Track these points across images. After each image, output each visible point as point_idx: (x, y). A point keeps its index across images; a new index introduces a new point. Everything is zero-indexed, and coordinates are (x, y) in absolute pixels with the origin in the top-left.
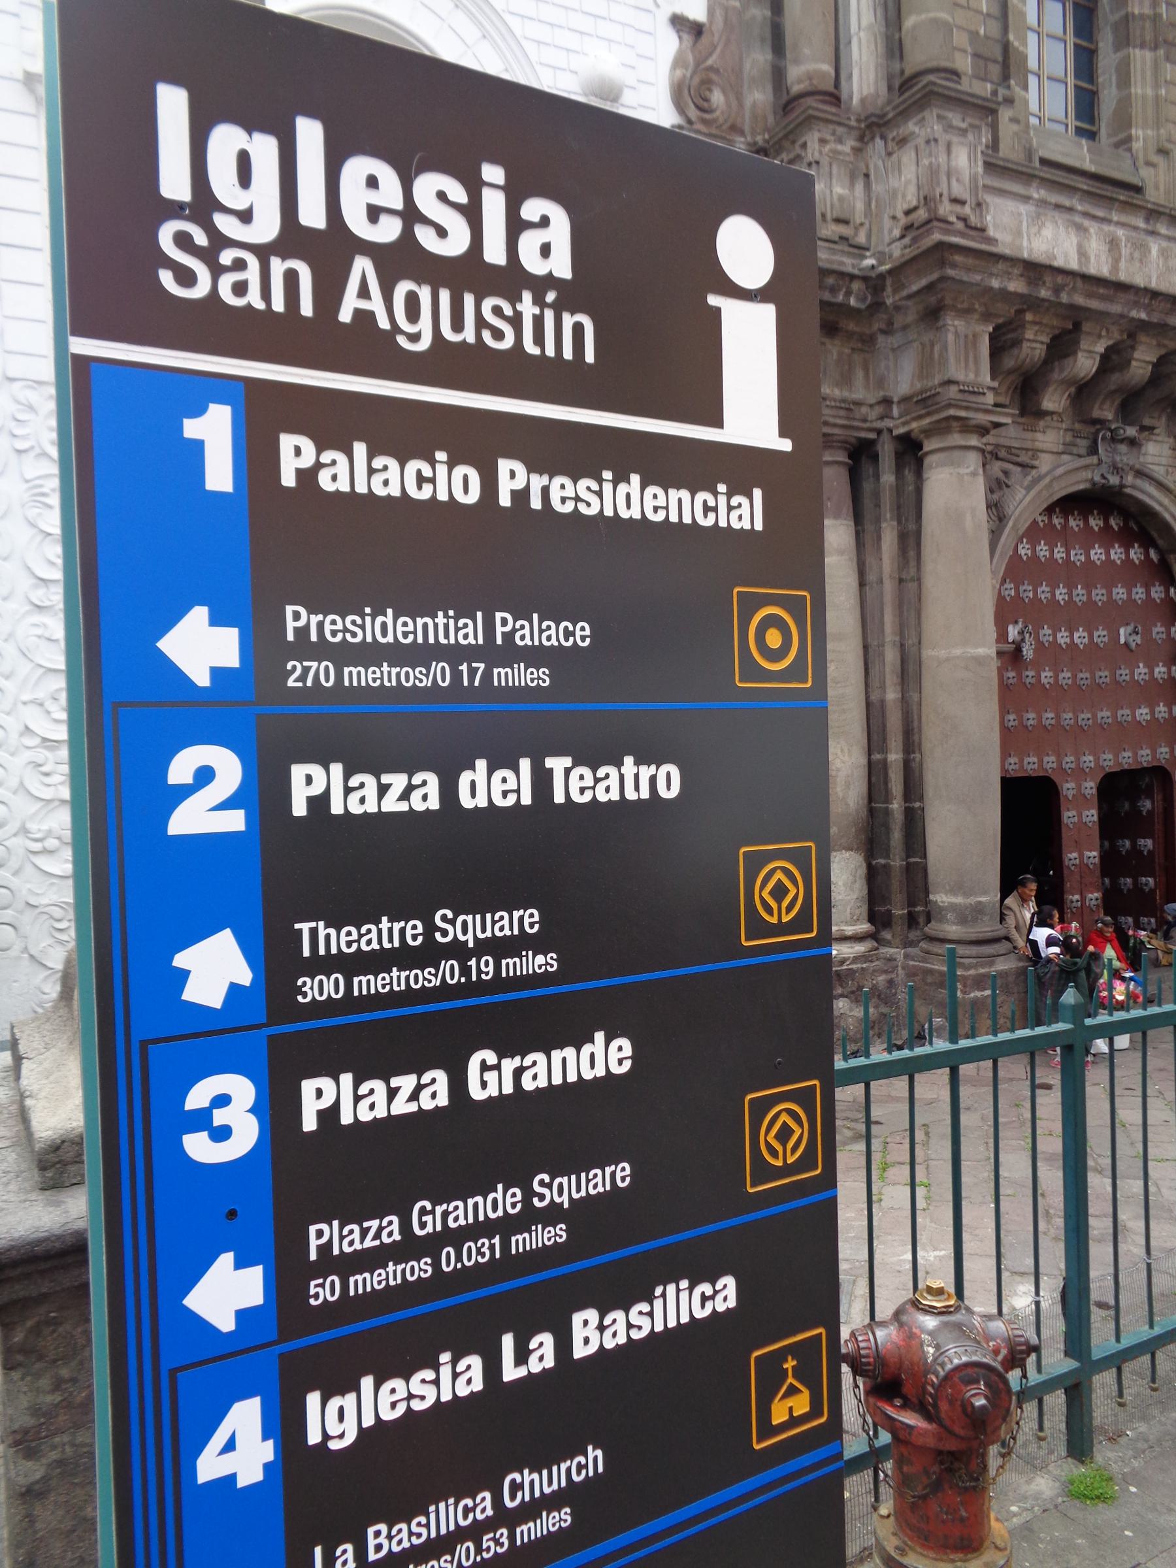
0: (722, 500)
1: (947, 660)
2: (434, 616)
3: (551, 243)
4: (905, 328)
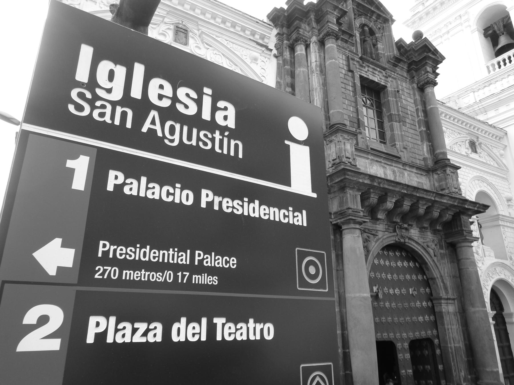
0: (291, 213)
1: (355, 297)
2: (168, 250)
3: (228, 116)
4: (334, 192)
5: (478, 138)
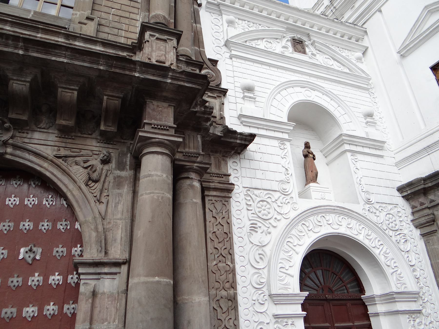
5: (308, 35)
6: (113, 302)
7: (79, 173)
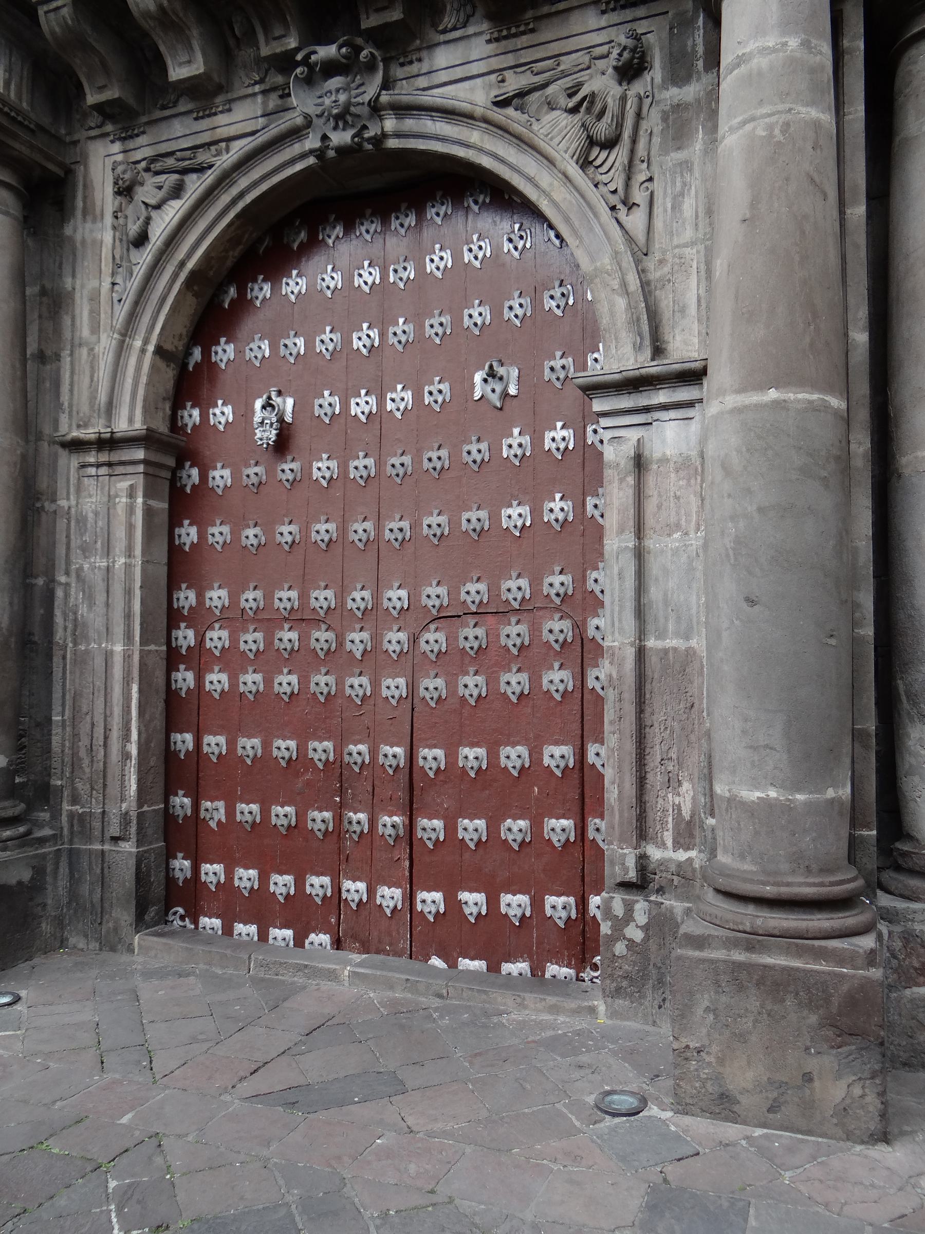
6: (693, 482)
7: (558, 131)
